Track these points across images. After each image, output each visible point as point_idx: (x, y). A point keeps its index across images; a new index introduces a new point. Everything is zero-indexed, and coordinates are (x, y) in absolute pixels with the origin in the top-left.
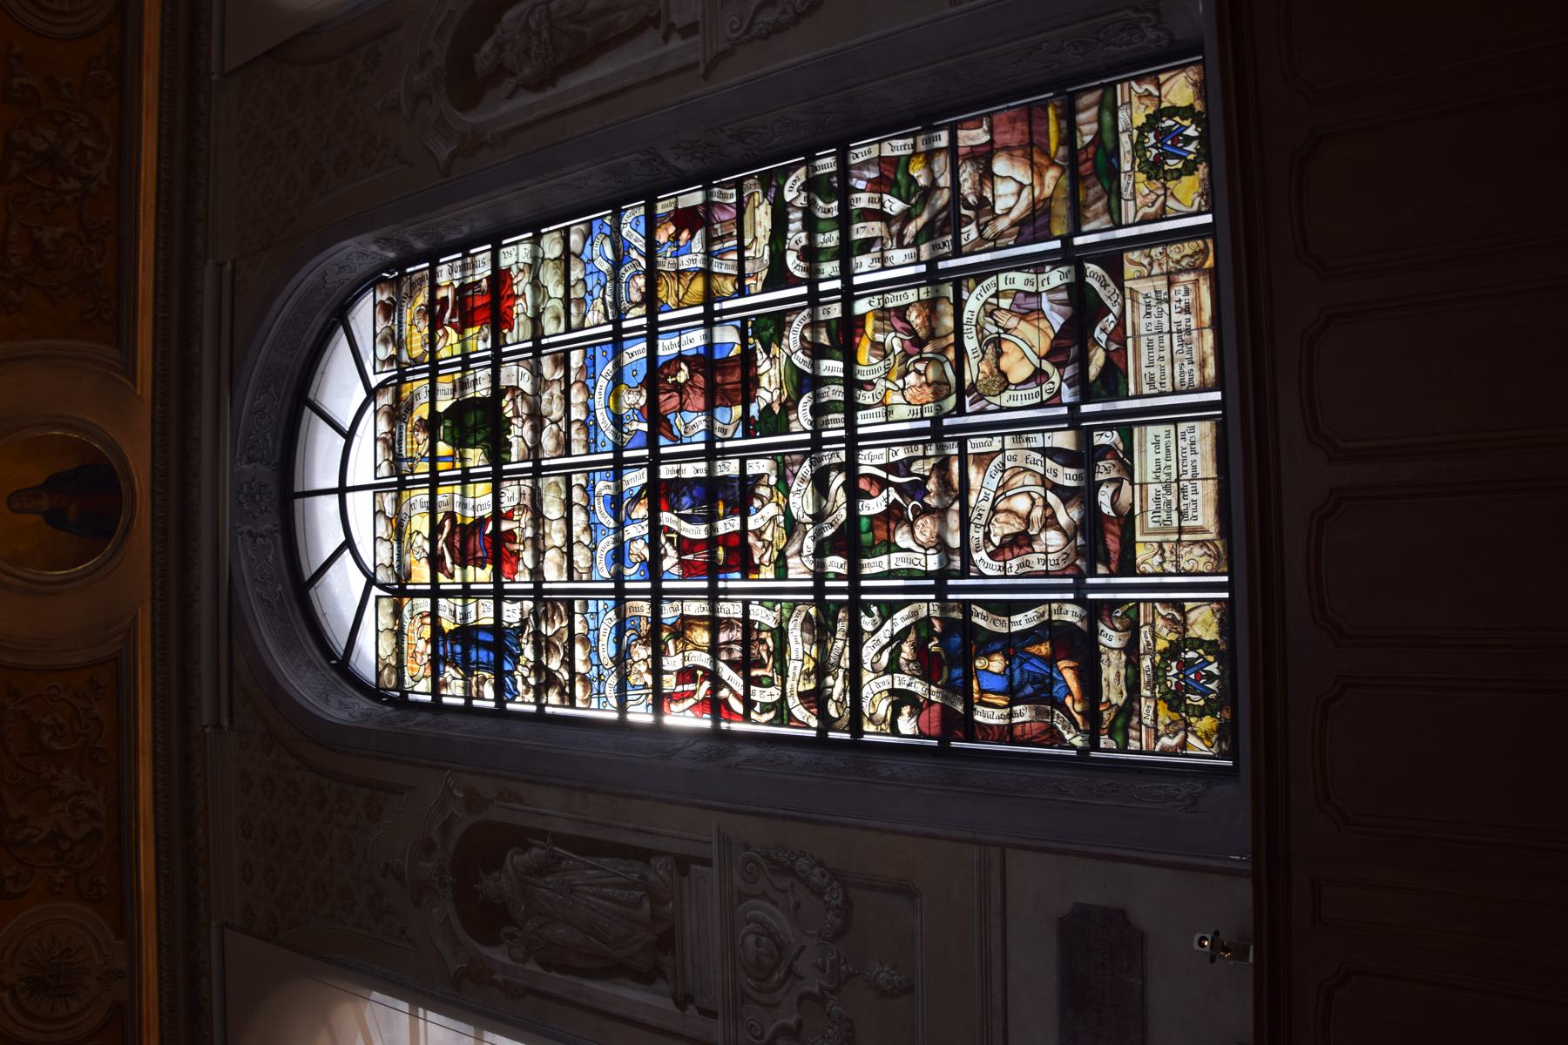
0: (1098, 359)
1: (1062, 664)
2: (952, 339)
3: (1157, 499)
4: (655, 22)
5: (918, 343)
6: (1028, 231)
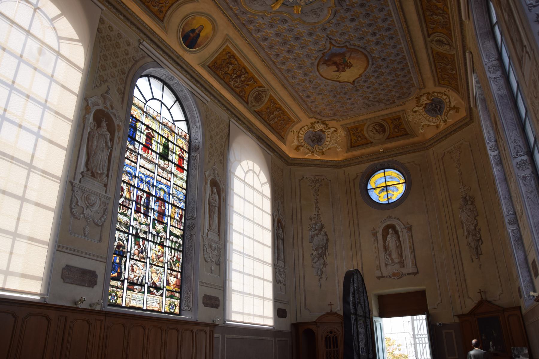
0: (152, 289)
1: (116, 274)
3: (135, 296)
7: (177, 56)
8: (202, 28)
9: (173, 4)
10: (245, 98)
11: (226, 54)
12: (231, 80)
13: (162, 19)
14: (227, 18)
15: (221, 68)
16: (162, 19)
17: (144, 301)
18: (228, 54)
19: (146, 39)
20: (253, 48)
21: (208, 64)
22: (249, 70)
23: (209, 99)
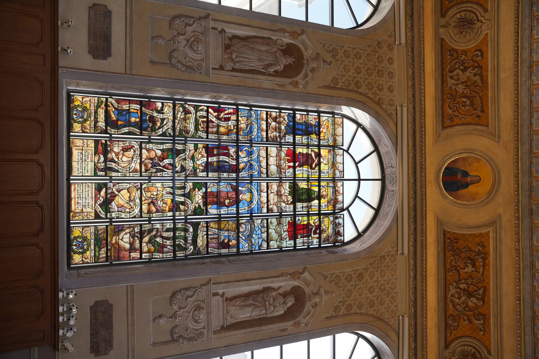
0: (103, 193)
1: (115, 119)
2: (143, 203)
3: (88, 157)
4: (227, 299)
5: (152, 202)
6: (120, 228)
7: (421, 164)
8: (478, 180)
9: (470, 124)
10: (451, 333)
11: (478, 244)
12: (455, 285)
13: (445, 126)
14: (516, 186)
15: (457, 255)
16: (445, 126)
17: (82, 176)
18: (481, 246)
19: (411, 115)
20: (519, 265)
21: (447, 229)
22: (489, 299)
23: (406, 251)
